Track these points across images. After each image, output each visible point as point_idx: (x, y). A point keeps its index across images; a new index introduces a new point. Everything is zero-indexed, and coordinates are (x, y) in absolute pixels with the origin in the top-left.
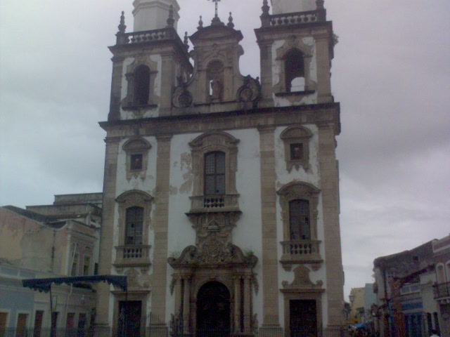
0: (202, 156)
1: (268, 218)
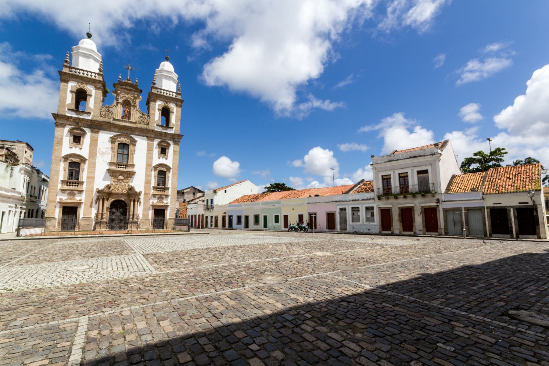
0: (117, 144)
1: (148, 176)
